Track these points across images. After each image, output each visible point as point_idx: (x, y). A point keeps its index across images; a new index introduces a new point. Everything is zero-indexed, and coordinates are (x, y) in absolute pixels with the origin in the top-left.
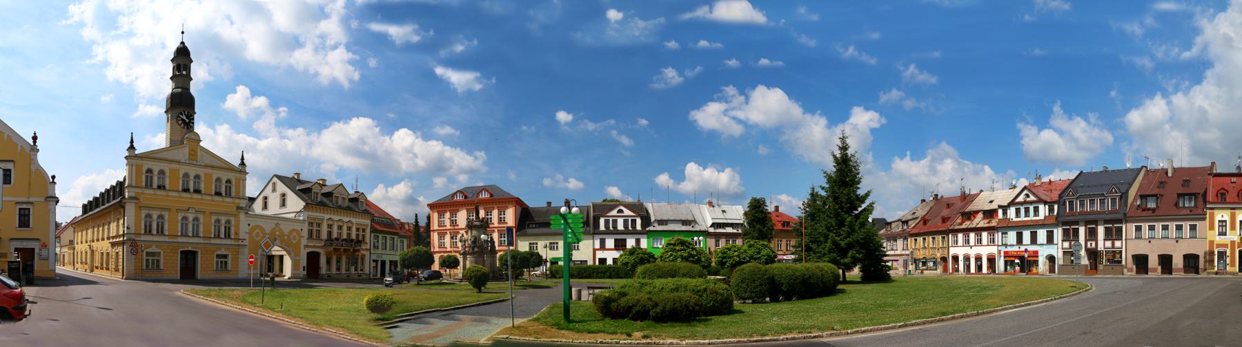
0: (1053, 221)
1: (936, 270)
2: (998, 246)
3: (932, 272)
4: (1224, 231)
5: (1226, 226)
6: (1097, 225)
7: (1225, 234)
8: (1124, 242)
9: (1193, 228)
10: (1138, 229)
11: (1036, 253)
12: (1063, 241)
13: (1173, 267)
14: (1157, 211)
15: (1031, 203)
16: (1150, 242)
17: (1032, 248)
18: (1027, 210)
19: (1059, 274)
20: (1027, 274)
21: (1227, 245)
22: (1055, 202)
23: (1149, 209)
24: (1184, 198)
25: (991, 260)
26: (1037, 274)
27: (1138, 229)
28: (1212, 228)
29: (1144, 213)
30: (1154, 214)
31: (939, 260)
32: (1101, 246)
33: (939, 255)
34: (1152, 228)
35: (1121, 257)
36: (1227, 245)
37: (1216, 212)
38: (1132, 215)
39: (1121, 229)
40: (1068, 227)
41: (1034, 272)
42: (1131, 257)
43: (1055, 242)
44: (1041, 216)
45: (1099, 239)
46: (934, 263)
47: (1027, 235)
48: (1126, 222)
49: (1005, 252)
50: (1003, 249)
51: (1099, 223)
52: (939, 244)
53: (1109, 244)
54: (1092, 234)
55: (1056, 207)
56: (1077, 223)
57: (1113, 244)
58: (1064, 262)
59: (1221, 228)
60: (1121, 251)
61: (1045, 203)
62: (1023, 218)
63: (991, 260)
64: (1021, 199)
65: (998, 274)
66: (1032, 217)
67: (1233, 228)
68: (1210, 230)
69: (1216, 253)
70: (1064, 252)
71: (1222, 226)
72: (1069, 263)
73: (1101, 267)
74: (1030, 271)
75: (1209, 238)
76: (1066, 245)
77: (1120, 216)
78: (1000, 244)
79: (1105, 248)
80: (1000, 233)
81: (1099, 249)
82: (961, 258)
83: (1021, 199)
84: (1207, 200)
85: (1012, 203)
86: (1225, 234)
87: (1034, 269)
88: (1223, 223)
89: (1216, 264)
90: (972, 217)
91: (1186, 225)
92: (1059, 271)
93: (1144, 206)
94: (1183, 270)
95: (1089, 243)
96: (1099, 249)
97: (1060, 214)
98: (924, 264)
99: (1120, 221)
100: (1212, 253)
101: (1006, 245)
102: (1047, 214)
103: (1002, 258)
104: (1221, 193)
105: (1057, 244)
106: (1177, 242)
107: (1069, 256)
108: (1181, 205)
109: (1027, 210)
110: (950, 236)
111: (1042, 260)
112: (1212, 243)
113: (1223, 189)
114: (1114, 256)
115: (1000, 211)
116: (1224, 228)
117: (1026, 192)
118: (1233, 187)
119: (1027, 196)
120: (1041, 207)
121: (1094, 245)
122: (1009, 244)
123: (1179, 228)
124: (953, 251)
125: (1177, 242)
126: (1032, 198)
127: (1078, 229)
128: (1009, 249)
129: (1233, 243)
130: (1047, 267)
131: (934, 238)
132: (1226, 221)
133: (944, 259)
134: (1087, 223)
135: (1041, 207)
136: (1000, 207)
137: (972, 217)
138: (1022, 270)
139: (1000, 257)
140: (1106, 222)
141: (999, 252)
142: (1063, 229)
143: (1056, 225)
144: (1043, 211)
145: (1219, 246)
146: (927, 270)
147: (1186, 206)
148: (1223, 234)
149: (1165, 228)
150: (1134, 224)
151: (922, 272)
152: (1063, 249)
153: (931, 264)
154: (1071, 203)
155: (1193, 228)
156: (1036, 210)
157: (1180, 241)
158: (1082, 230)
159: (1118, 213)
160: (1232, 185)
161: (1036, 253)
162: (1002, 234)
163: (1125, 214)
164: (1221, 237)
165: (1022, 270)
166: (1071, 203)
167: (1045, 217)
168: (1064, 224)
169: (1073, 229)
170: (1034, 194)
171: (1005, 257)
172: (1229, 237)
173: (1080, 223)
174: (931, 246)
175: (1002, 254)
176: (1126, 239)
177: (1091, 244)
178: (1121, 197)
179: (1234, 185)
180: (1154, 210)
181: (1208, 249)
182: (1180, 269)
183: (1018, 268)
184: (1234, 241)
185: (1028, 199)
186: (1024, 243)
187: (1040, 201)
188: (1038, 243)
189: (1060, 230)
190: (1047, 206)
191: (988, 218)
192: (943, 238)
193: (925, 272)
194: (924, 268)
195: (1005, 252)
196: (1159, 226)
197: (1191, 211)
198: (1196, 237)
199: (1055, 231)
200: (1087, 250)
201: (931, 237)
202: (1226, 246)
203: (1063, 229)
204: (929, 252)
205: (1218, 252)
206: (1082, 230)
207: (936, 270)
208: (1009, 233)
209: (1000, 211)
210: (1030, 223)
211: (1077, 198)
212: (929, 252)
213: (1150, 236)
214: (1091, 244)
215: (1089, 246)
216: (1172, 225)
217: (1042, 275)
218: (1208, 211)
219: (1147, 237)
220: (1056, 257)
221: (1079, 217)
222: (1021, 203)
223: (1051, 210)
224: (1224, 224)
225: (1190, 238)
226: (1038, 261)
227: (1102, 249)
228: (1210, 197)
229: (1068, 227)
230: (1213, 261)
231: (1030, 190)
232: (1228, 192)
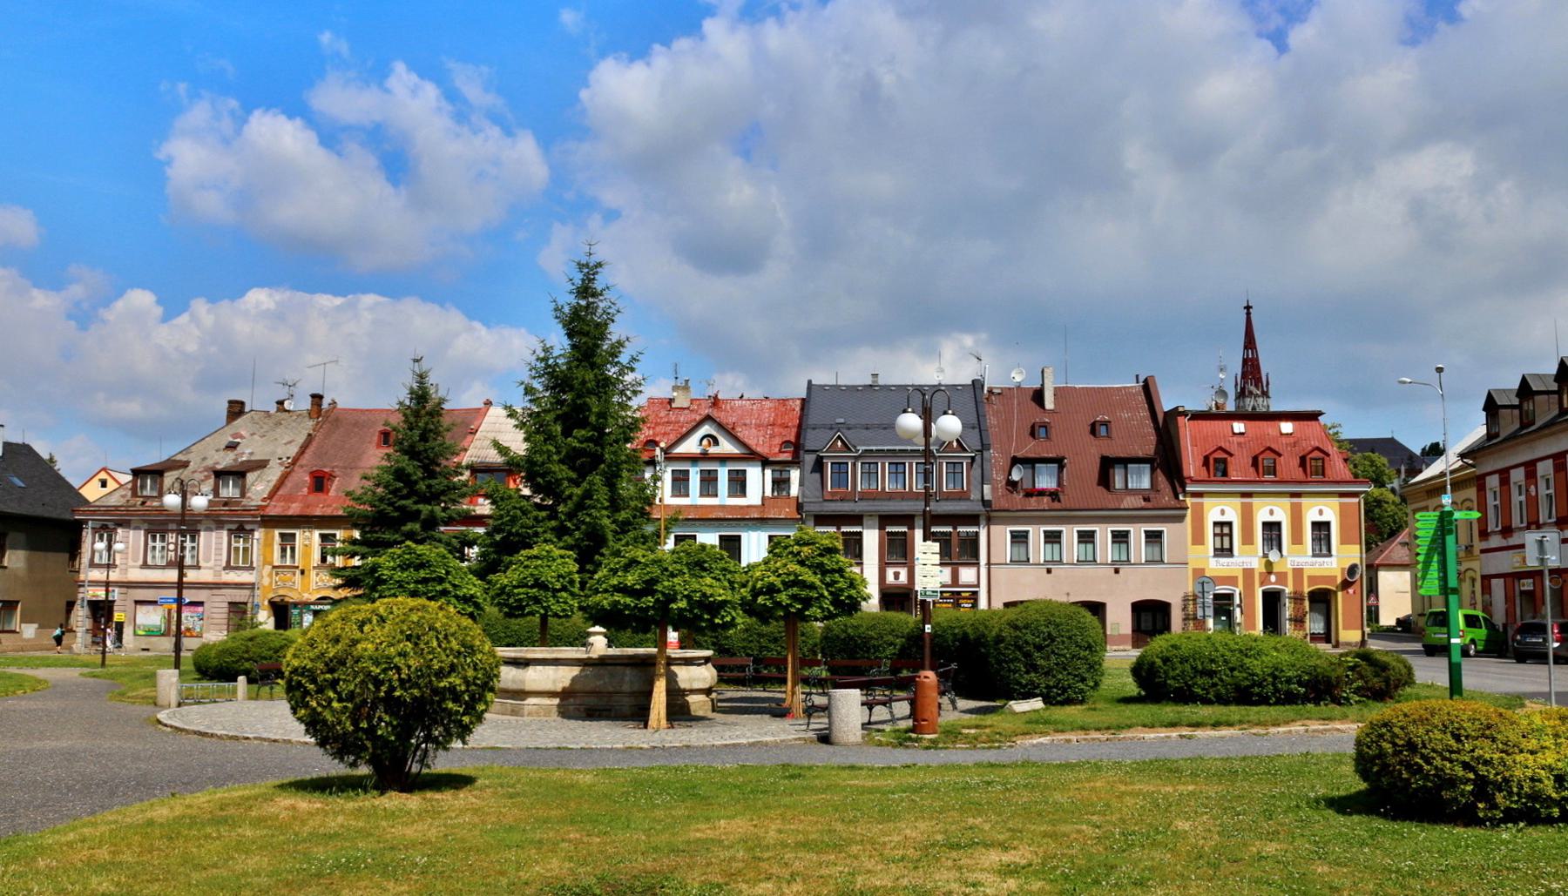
4: (1227, 545)
5: (1230, 535)
6: (912, 528)
9: (1154, 538)
10: (1020, 539)
15: (723, 459)
16: (1049, 571)
18: (709, 482)
23: (1042, 493)
24: (1126, 468)
27: (1020, 539)
28: (1198, 539)
29: (1033, 502)
34: (1053, 538)
37: (1207, 502)
38: (1004, 504)
39: (974, 541)
44: (753, 496)
48: (989, 521)
54: (896, 550)
55: (795, 475)
56: (857, 519)
59: (1218, 539)
60: (975, 593)
61: (765, 463)
66: (724, 497)
67: (1248, 539)
68: (1193, 544)
71: (1222, 535)
84: (1185, 474)
88: (1223, 527)
91: (1137, 532)
93: (1027, 485)
95: (890, 572)
99: (972, 519)
102: (768, 493)
104: (1216, 460)
106: (1117, 571)
108: (1119, 484)
109: (709, 482)
113: (1221, 448)
116: (1226, 540)
117: (706, 429)
118: (1239, 444)
120: (754, 474)
121: (903, 578)
123: (1120, 538)
125: (1117, 571)
126: (726, 447)
127: (860, 534)
132: (1230, 524)
134: (885, 520)
135: (754, 474)
144: (758, 481)
147: (1130, 486)
149: (1086, 538)
155: (1154, 538)
156: (738, 484)
157: (1124, 569)
158: (871, 539)
159: (968, 499)
160: (1236, 439)
167: (763, 498)
176: (989, 564)
177: (897, 575)
179: (1241, 439)
180: (1054, 495)
185: (713, 450)
187: (751, 456)
190: (768, 472)
196: (1070, 533)
197: (1146, 499)
198: (1162, 561)
206: (871, 539)
210: (721, 515)
213: (1049, 558)
214: (897, 575)
215: (890, 578)
216: (1104, 532)
218: (1189, 501)
219: (1042, 562)
222: (693, 459)
223: (780, 483)
225: (1148, 562)
228: (1191, 466)
231: (721, 426)
232: (1231, 455)
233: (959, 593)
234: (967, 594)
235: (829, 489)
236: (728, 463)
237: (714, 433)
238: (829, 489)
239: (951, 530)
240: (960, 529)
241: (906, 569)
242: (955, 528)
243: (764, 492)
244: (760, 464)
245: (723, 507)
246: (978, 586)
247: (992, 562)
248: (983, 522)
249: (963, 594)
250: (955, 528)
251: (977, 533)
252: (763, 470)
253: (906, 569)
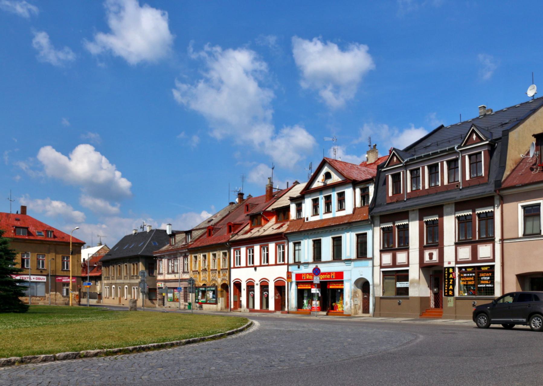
0: (365, 215)
1: (216, 303)
2: (288, 265)
3: (212, 305)
6: (441, 216)
8: (498, 246)
11: (340, 275)
12: (381, 251)
15: (334, 186)
17: (337, 267)
19: (374, 315)
20: (327, 315)
22: (368, 181)
25: (280, 289)
26: (341, 314)
31: (219, 288)
32: (449, 260)
33: (219, 282)
35: (492, 280)
39: (490, 217)
40: (390, 225)
41: (340, 309)
42: (515, 278)
43: (369, 255)
44: (349, 209)
45: (445, 243)
46: (215, 292)
47: (327, 243)
48: (503, 200)
49: (298, 276)
50: (295, 270)
51: (446, 210)
52: (219, 265)
53: (465, 252)
55: (372, 189)
56: (404, 215)
57: (474, 253)
58: (383, 292)
60: (493, 266)
61: (355, 184)
62: (322, 216)
63: (280, 289)
64: (318, 183)
65: (288, 312)
66: (335, 213)
70: (383, 272)
72: (392, 293)
73: (450, 302)
74: (333, 308)
76: (387, 258)
77: (489, 189)
78: (291, 261)
79: (457, 262)
80: (291, 244)
81: (446, 265)
82: (244, 286)
83: (318, 183)
85: (307, 191)
87: (339, 305)
90: (263, 221)
92: (374, 310)
95: (427, 253)
96: (446, 265)
97: (379, 201)
98: (204, 293)
99: (488, 201)
101: (298, 264)
102: (358, 205)
103: (294, 286)
105: (372, 259)
107: (394, 281)
110: (232, 251)
111: (348, 287)
114: (478, 279)
115: (293, 208)
117: (326, 169)
119: (328, 176)
120: (349, 192)
121: (435, 258)
122: (302, 261)
124: (236, 274)
126: (335, 178)
128: (303, 270)
130: (359, 302)
131: (214, 255)
133: (225, 287)
135: (349, 192)
136: (292, 199)
137: (263, 221)
138: (323, 307)
139: (291, 283)
140: (460, 205)
141: (289, 274)
142: (383, 229)
143: (370, 222)
146: (206, 303)
150: (520, 205)
151: (201, 307)
152: (381, 267)
153: (210, 295)
154: (396, 178)
158: (414, 228)
161: (340, 275)
162: (295, 244)
163: (498, 184)
165: (323, 307)
166: (396, 178)
167: (355, 209)
168: (384, 218)
169: (398, 226)
170: (339, 173)
171: (298, 284)
173: (411, 215)
174: (211, 267)
175: (294, 279)
176: (502, 240)
177: (431, 255)
178: (491, 149)
183: (316, 303)
185: (329, 182)
186: (323, 259)
188: (343, 258)
189: (377, 231)
190: (358, 191)
191: (280, 222)
192: (225, 254)
193: (205, 306)
194: (204, 300)
195: (298, 276)
199: (369, 233)
200: (424, 267)
201: (211, 254)
203: (383, 229)
204: (209, 276)
206: (414, 228)
207: (216, 303)
208: (302, 242)
209: (293, 208)
211: (406, 166)
212: (209, 276)
214: (431, 255)
215: (427, 258)
217: (349, 316)
220: (371, 283)
221: (409, 203)
222: (320, 190)
223: (365, 196)
226: (342, 290)
227: (453, 264)
229: (390, 225)
231: (331, 166)
233: (479, 267)
234: (486, 268)
235: (390, 194)
236: (336, 189)
237: (330, 171)
238: (390, 194)
239: (471, 213)
240: (478, 211)
241: (437, 250)
242: (474, 211)
243: (355, 205)
244: (351, 185)
245: (334, 219)
246: (493, 260)
247: (505, 237)
248: (497, 202)
249: (483, 269)
250: (474, 211)
251: (493, 213)
252: (354, 189)
253: (437, 250)
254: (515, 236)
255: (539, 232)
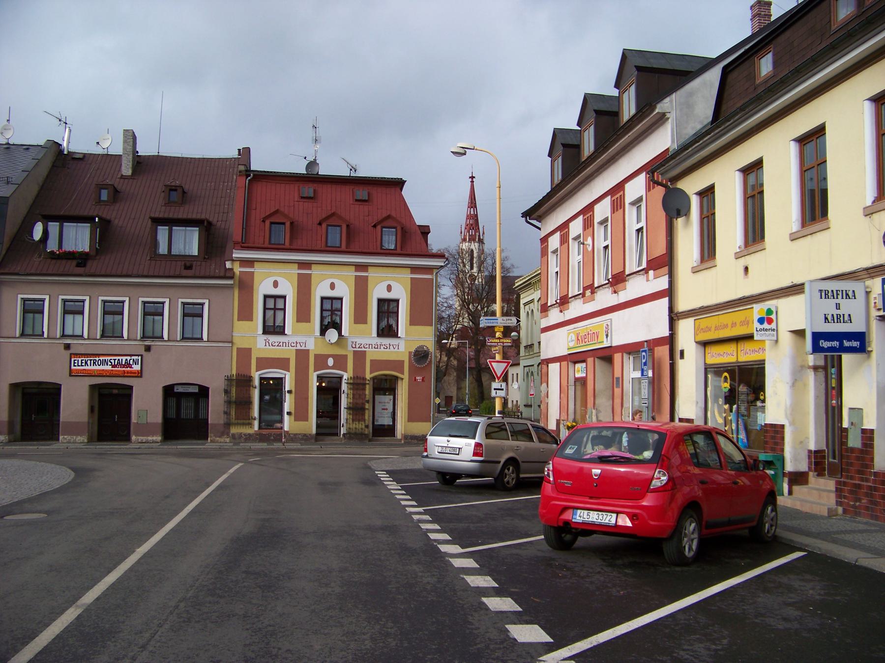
4: (279, 322)
7: (280, 331)
9: (192, 313)
13: (134, 419)
14: (89, 263)
21: (288, 360)
28: (246, 314)
30: (80, 270)
36: (288, 360)
59: (270, 313)
67: (303, 315)
69: (257, 382)
75: (240, 342)
86: (280, 331)
88: (275, 302)
89: (256, 412)
94: (160, 429)
100: (244, 381)
112: (245, 354)
116: (280, 314)
129: (302, 355)
145: (264, 363)
148: (273, 329)
155: (192, 313)
164: (273, 339)
172: (293, 339)
181: (234, 372)
182: (154, 425)
184: (308, 350)
202: (283, 363)
205: (261, 379)
224: (280, 304)
230: (249, 403)
254: (14, 336)
255: (41, 333)
